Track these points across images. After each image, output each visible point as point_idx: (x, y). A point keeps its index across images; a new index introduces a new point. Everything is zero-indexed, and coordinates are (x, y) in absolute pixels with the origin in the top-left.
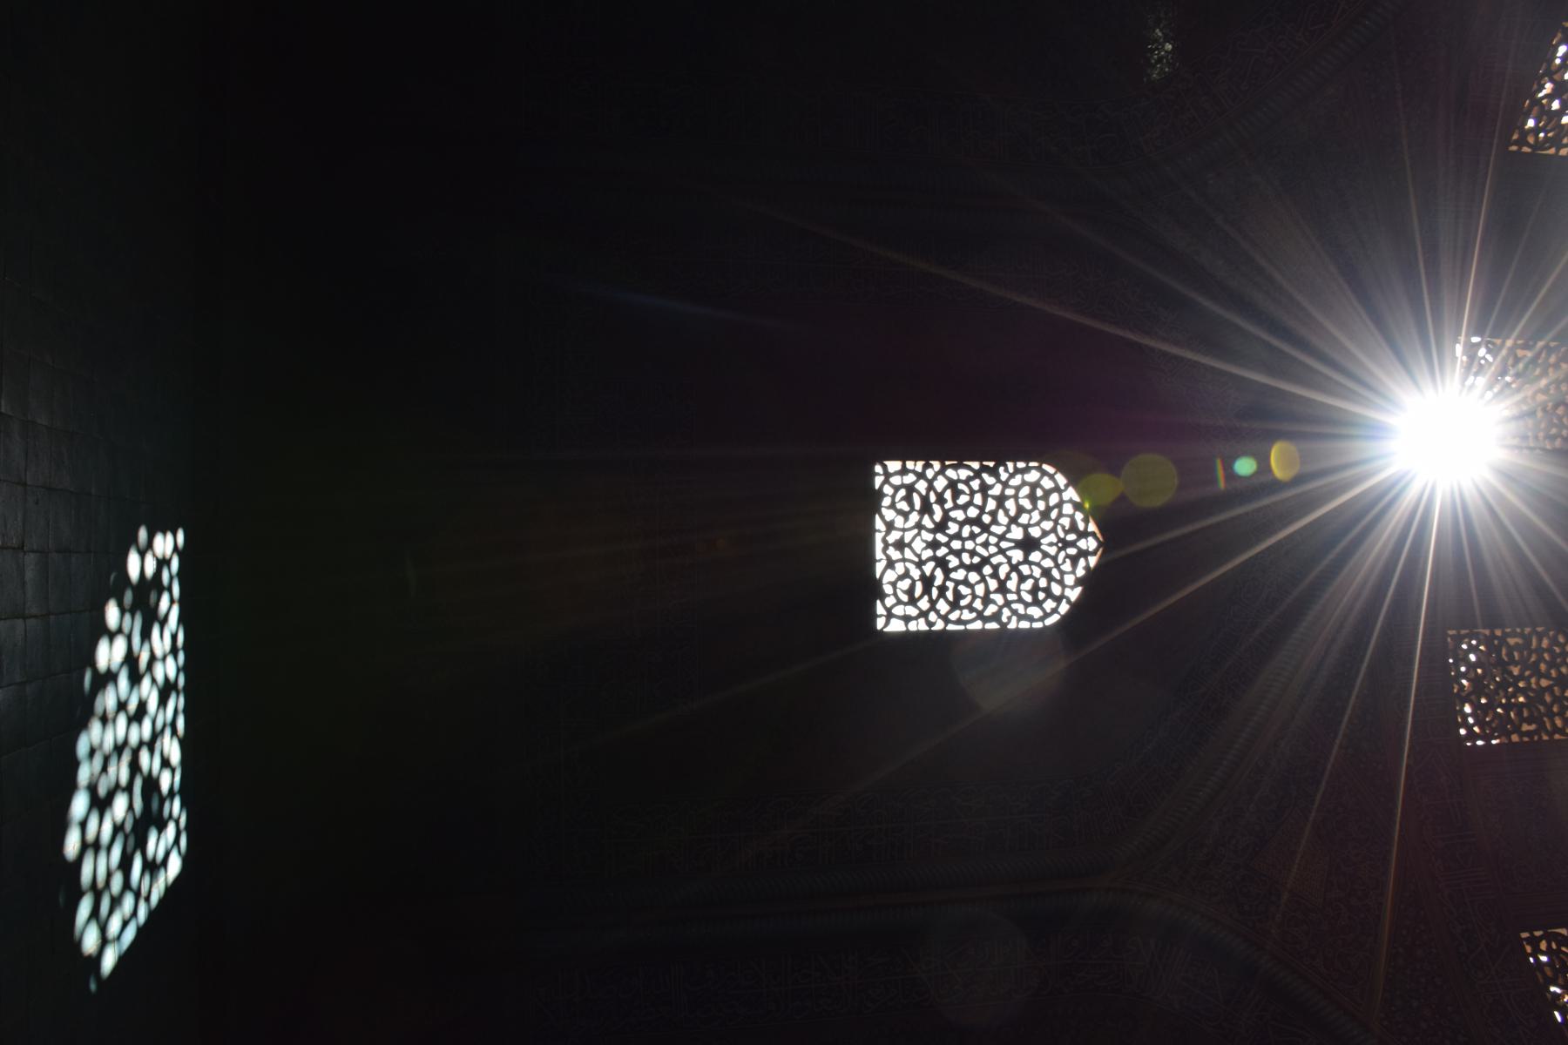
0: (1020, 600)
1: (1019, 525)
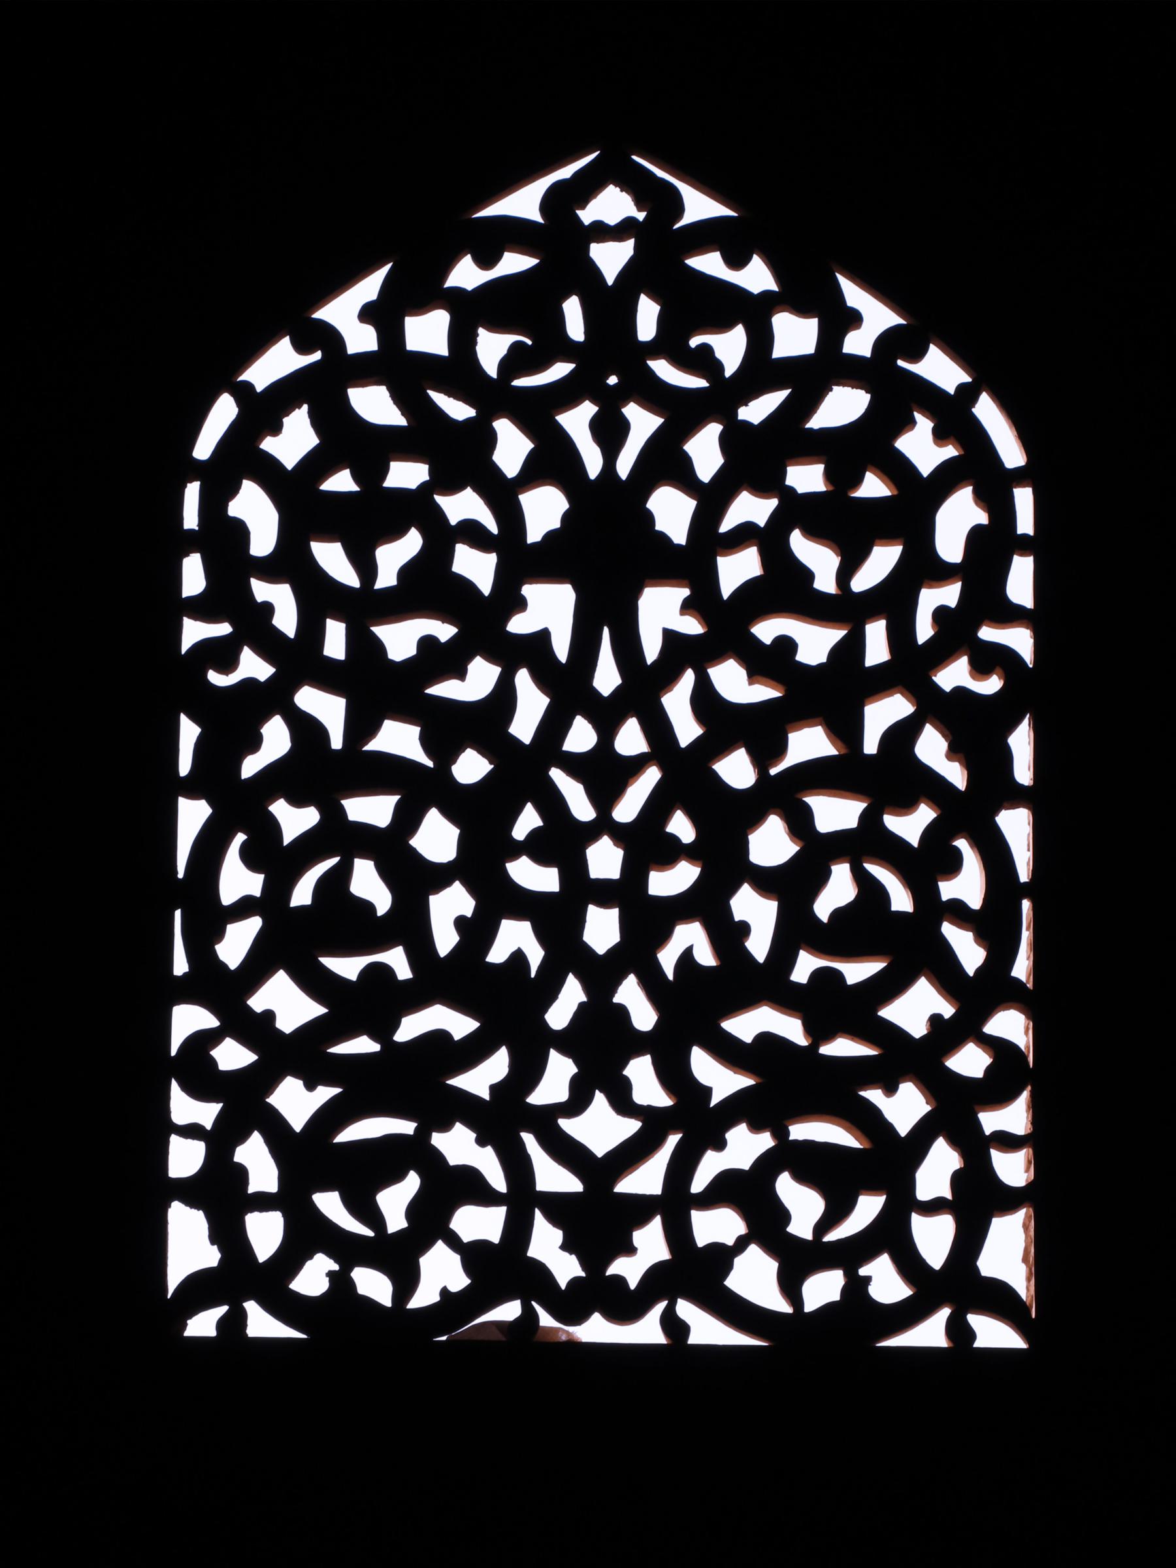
0: (894, 599)
1: (509, 598)
